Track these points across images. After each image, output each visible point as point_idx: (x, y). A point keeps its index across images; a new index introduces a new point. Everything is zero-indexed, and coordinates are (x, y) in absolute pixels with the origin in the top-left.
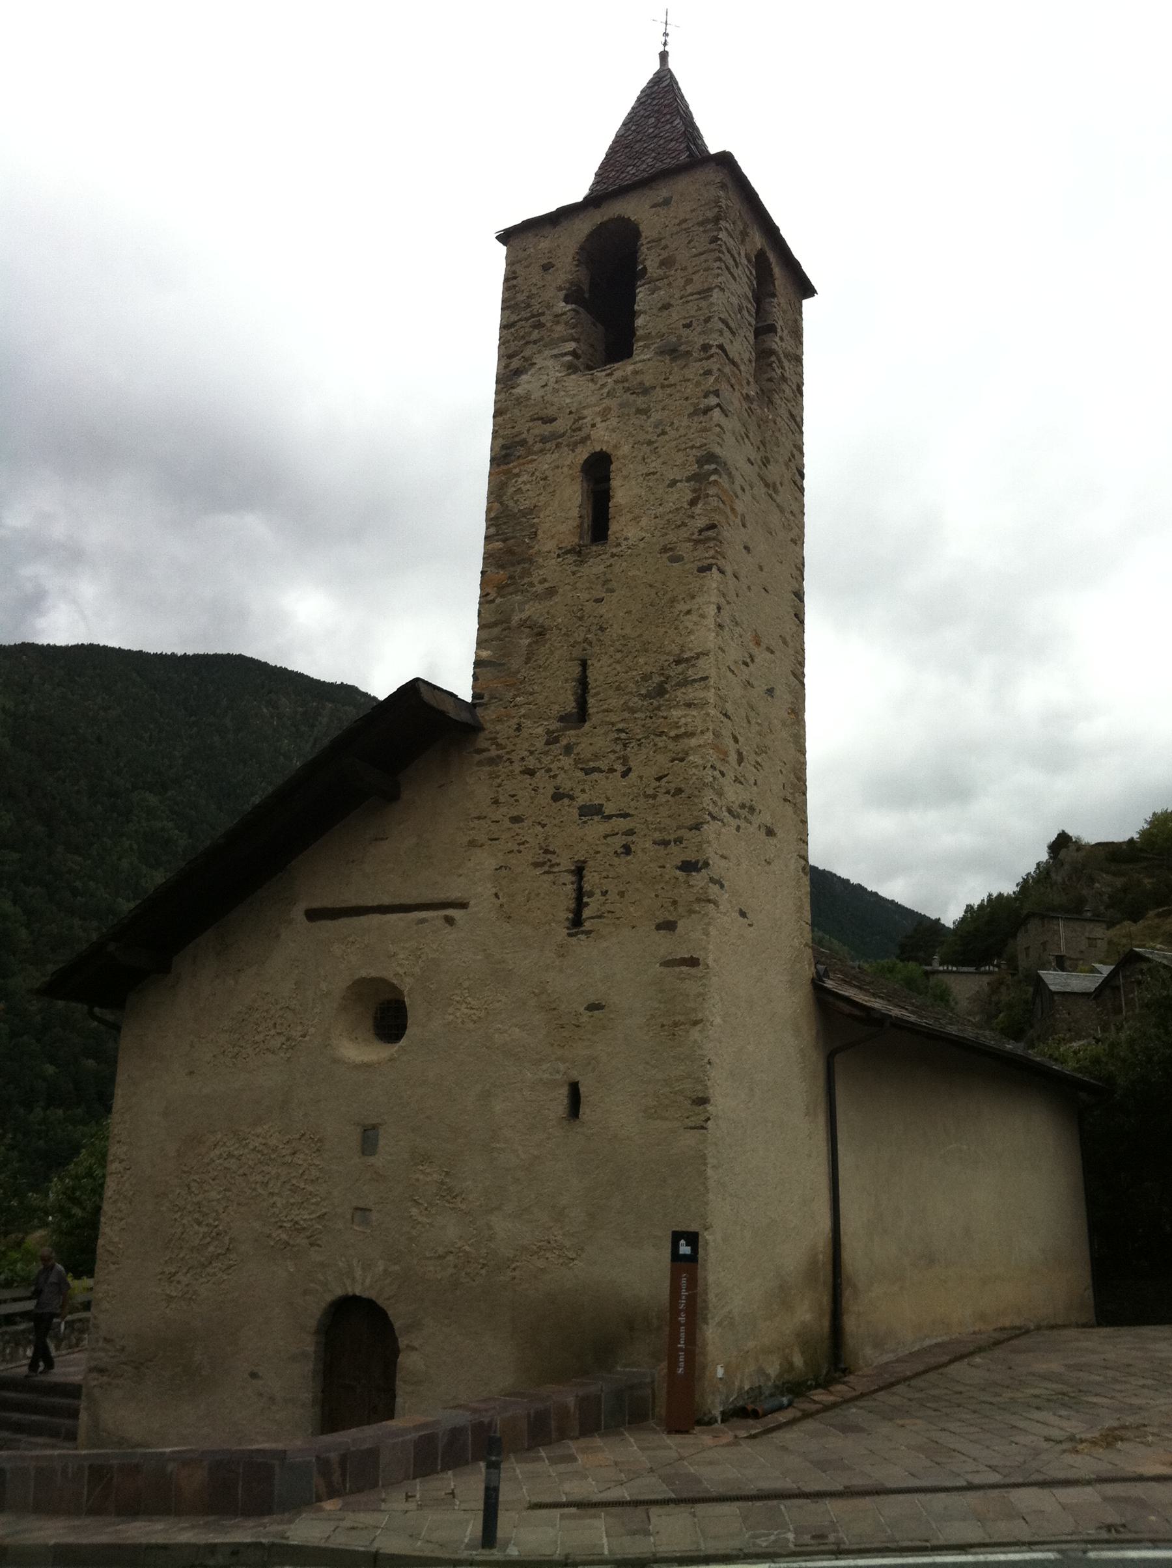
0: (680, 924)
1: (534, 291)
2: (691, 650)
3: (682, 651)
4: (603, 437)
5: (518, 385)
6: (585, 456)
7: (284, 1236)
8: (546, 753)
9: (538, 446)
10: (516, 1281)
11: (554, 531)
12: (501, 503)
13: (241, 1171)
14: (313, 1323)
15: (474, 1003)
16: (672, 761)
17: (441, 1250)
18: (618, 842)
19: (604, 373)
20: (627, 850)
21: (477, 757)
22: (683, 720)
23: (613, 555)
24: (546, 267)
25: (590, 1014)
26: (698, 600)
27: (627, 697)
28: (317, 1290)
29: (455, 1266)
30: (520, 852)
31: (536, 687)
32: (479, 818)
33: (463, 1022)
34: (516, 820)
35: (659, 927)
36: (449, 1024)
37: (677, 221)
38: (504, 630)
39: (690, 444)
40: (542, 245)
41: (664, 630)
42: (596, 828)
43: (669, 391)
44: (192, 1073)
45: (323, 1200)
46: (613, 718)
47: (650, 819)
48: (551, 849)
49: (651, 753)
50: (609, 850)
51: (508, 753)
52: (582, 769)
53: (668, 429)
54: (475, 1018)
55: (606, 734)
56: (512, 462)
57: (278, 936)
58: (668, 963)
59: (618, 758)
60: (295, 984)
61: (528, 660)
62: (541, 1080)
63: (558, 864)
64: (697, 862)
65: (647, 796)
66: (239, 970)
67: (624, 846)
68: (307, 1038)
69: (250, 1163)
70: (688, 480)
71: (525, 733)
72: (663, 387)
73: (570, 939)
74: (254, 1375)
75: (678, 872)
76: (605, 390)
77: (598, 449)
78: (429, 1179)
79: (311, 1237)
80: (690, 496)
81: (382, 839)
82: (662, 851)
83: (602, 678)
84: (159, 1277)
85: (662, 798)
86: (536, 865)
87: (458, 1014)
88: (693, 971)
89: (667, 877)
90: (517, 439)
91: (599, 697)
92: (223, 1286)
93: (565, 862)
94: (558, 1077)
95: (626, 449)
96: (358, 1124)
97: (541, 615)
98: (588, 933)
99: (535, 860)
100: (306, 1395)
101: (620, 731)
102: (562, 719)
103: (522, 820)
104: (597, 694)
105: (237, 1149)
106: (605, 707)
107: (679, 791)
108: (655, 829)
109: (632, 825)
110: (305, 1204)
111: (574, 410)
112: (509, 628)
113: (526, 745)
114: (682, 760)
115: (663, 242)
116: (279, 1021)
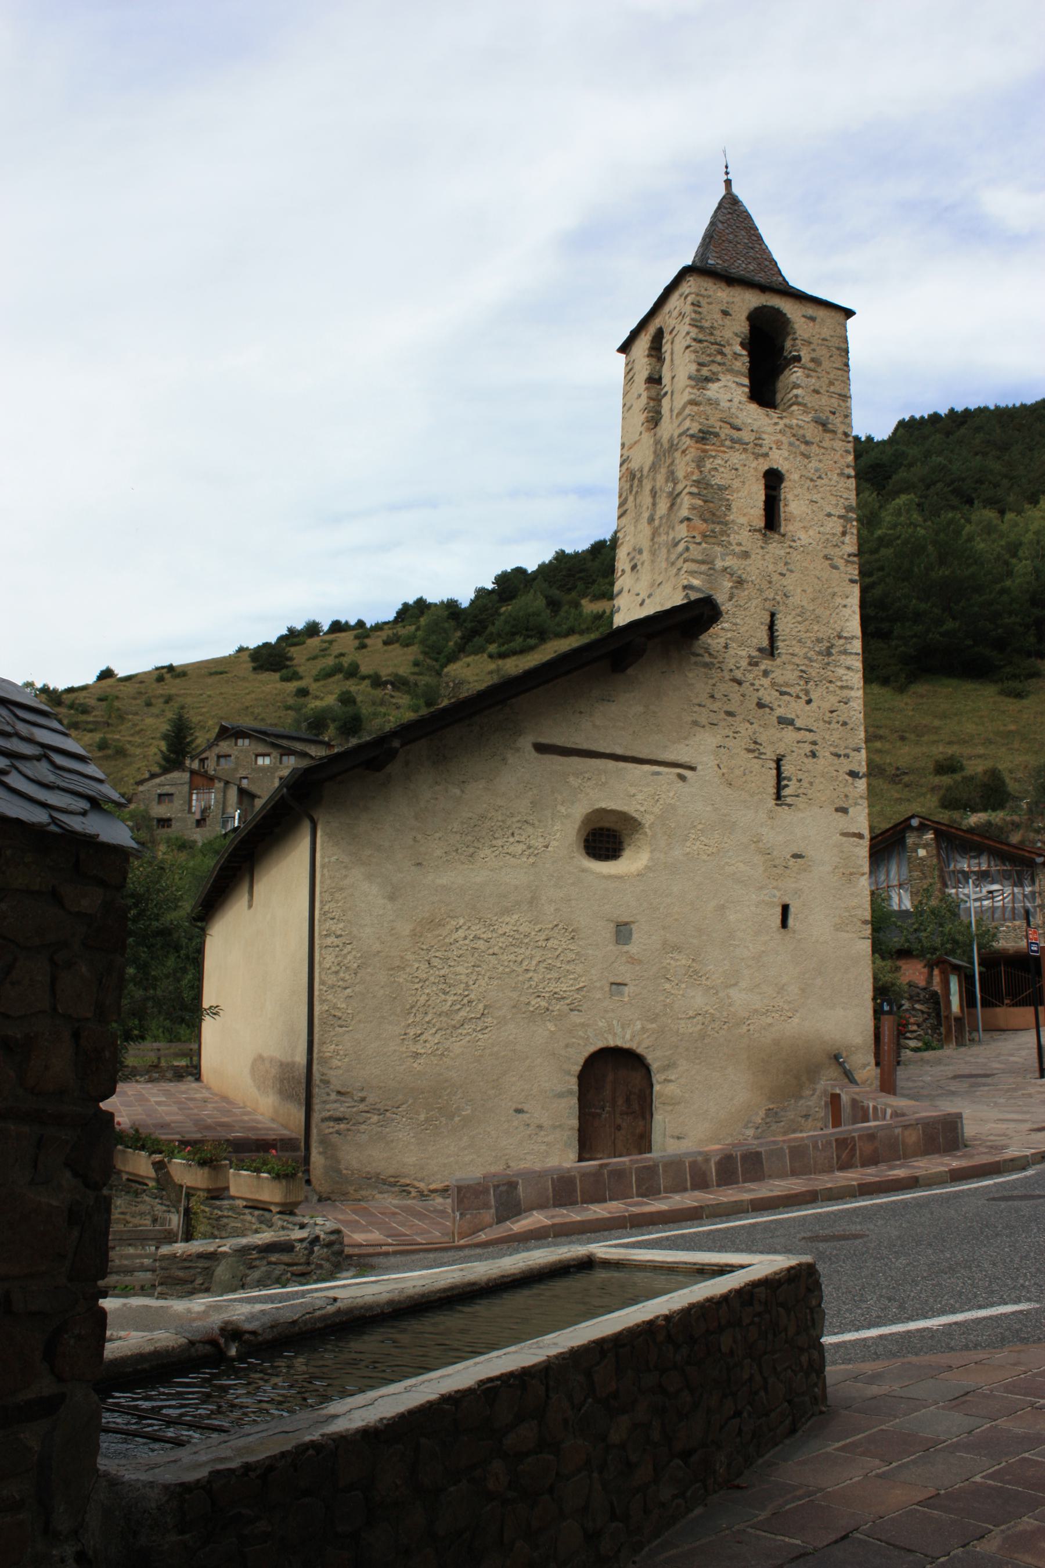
0: (851, 810)
1: (715, 325)
2: (848, 632)
3: (842, 631)
4: (779, 460)
5: (708, 390)
6: (766, 468)
7: (544, 1004)
8: (750, 671)
9: (728, 443)
10: (751, 1032)
11: (745, 511)
12: (701, 472)
13: (491, 951)
14: (577, 1068)
15: (707, 841)
16: (840, 702)
17: (691, 1013)
18: (807, 748)
19: (777, 415)
20: (814, 755)
21: (693, 659)
22: (844, 678)
23: (791, 547)
24: (725, 313)
25: (794, 860)
26: (849, 600)
27: (807, 649)
28: (579, 1044)
29: (703, 1024)
30: (735, 738)
31: (738, 621)
32: (700, 705)
33: (698, 854)
34: (730, 714)
35: (837, 810)
36: (688, 854)
37: (822, 337)
38: (710, 569)
39: (840, 494)
40: (719, 294)
41: (828, 612)
42: (789, 735)
43: (823, 451)
44: (419, 864)
45: (580, 976)
46: (796, 660)
47: (827, 737)
48: (759, 741)
49: (824, 692)
50: (800, 751)
51: (719, 662)
52: (777, 690)
53: (823, 476)
54: (709, 852)
55: (793, 670)
56: (708, 445)
57: (504, 760)
58: (845, 834)
59: (802, 690)
60: (531, 803)
61: (731, 599)
62: (763, 901)
63: (765, 754)
64: (858, 773)
65: (825, 722)
66: (463, 782)
67: (811, 751)
68: (550, 849)
69: (500, 945)
70: (840, 517)
71: (731, 652)
72: (819, 447)
73: (777, 807)
74: (519, 1111)
75: (847, 777)
76: (778, 428)
77: (775, 467)
78: (678, 963)
80: (841, 529)
81: (609, 701)
82: (836, 760)
83: (788, 630)
84: (402, 1037)
85: (834, 726)
86: (749, 751)
87: (695, 848)
88: (861, 841)
89: (840, 779)
90: (710, 430)
91: (786, 643)
92: (479, 1043)
93: (770, 754)
94: (775, 900)
95: (795, 476)
96: (612, 921)
97: (739, 569)
98: (789, 805)
99: (747, 747)
101: (802, 671)
102: (760, 650)
103: (734, 716)
104: (784, 640)
105: (484, 933)
106: (791, 651)
107: (845, 724)
108: (831, 745)
109: (815, 739)
110: (562, 979)
111: (755, 429)
112: (713, 569)
113: (733, 661)
114: (846, 703)
115: (812, 346)
116: (517, 832)
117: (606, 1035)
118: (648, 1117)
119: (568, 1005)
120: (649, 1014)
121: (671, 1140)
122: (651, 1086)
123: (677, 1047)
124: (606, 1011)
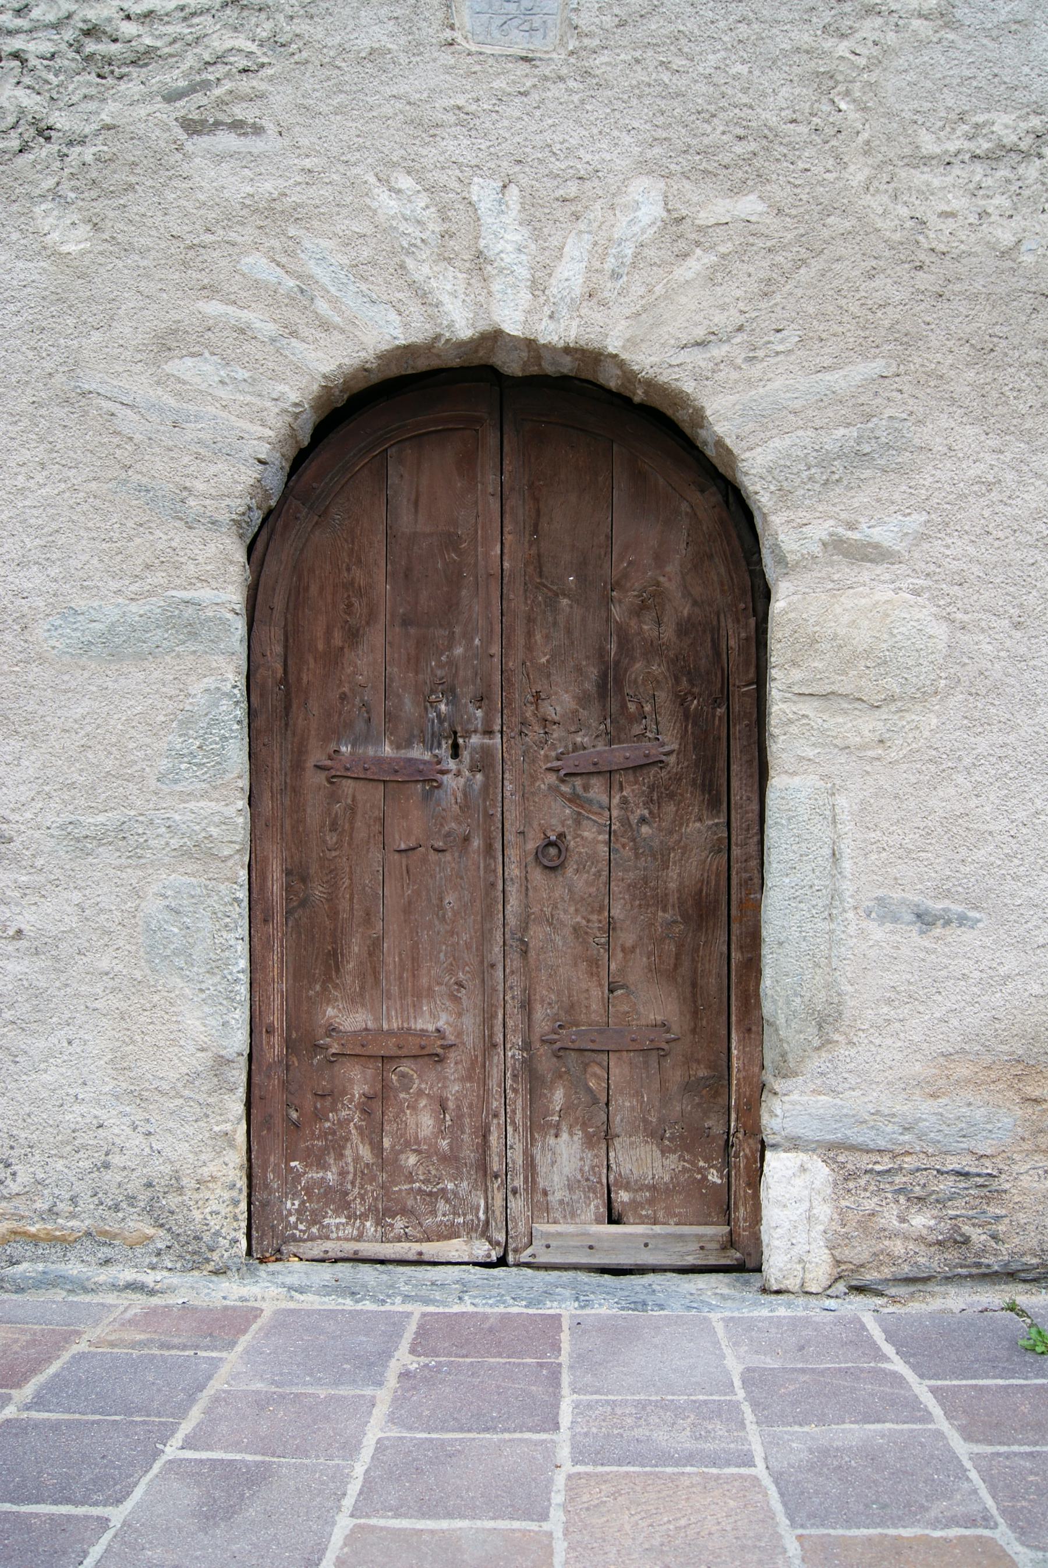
79: (192, 89)
100: (207, 806)
117: (421, 270)
118: (741, 791)
119: (171, 97)
120: (715, 133)
121: (877, 932)
122: (762, 594)
123: (908, 341)
124: (432, 129)
